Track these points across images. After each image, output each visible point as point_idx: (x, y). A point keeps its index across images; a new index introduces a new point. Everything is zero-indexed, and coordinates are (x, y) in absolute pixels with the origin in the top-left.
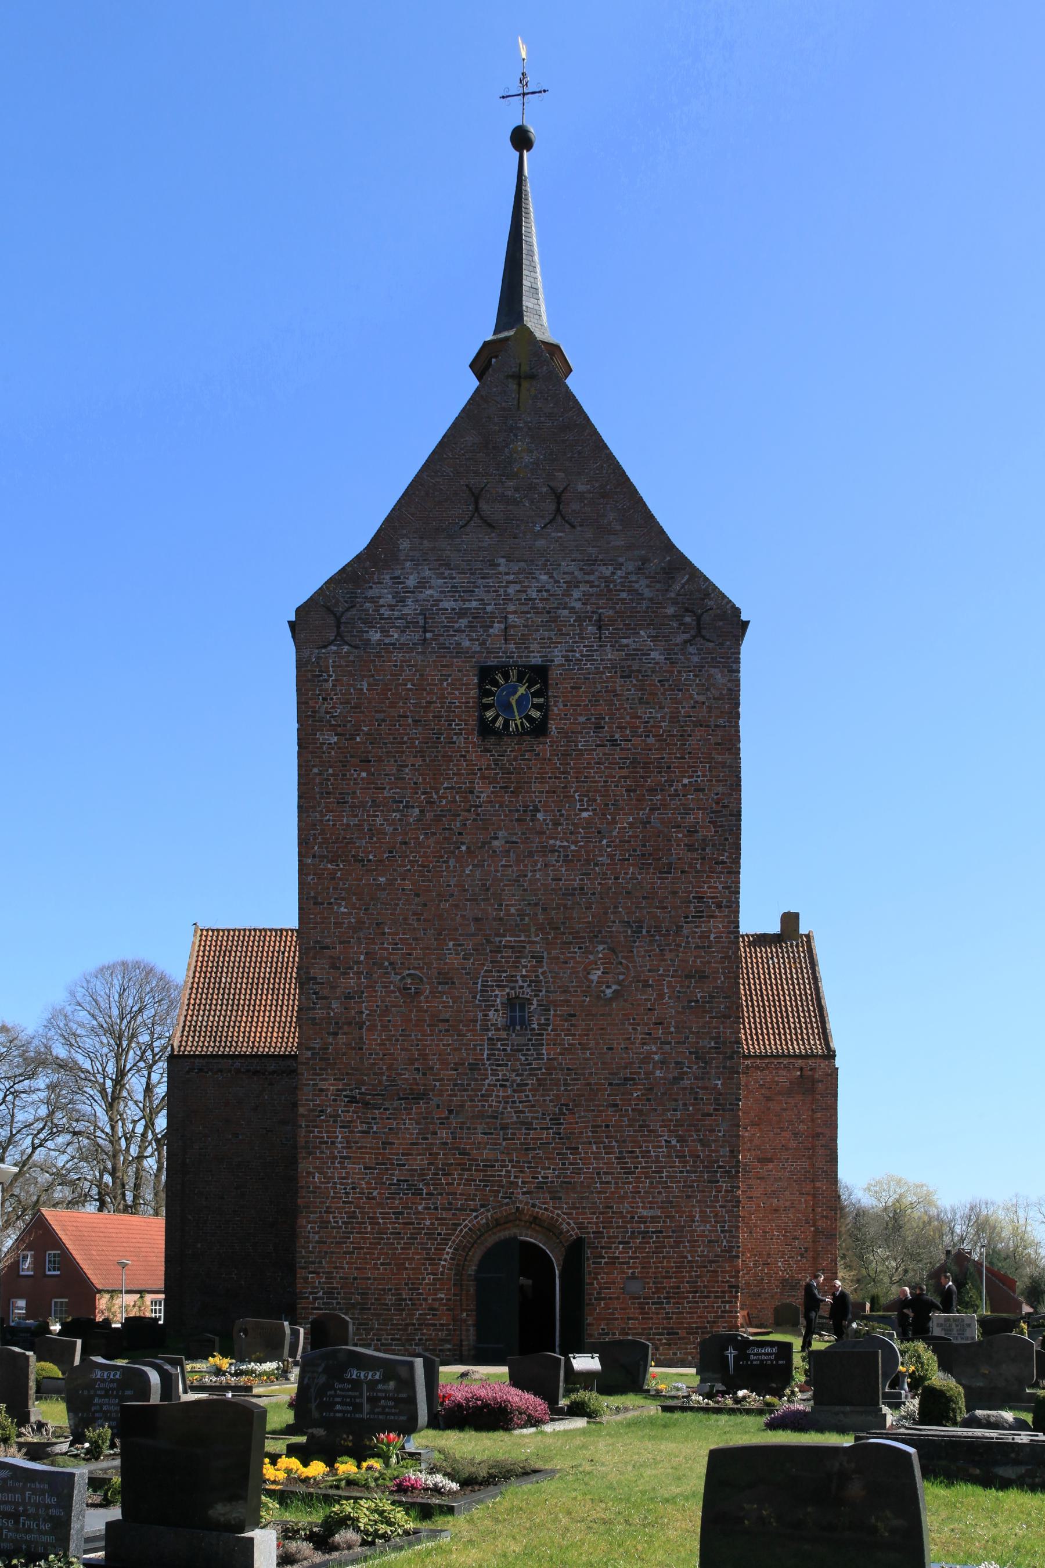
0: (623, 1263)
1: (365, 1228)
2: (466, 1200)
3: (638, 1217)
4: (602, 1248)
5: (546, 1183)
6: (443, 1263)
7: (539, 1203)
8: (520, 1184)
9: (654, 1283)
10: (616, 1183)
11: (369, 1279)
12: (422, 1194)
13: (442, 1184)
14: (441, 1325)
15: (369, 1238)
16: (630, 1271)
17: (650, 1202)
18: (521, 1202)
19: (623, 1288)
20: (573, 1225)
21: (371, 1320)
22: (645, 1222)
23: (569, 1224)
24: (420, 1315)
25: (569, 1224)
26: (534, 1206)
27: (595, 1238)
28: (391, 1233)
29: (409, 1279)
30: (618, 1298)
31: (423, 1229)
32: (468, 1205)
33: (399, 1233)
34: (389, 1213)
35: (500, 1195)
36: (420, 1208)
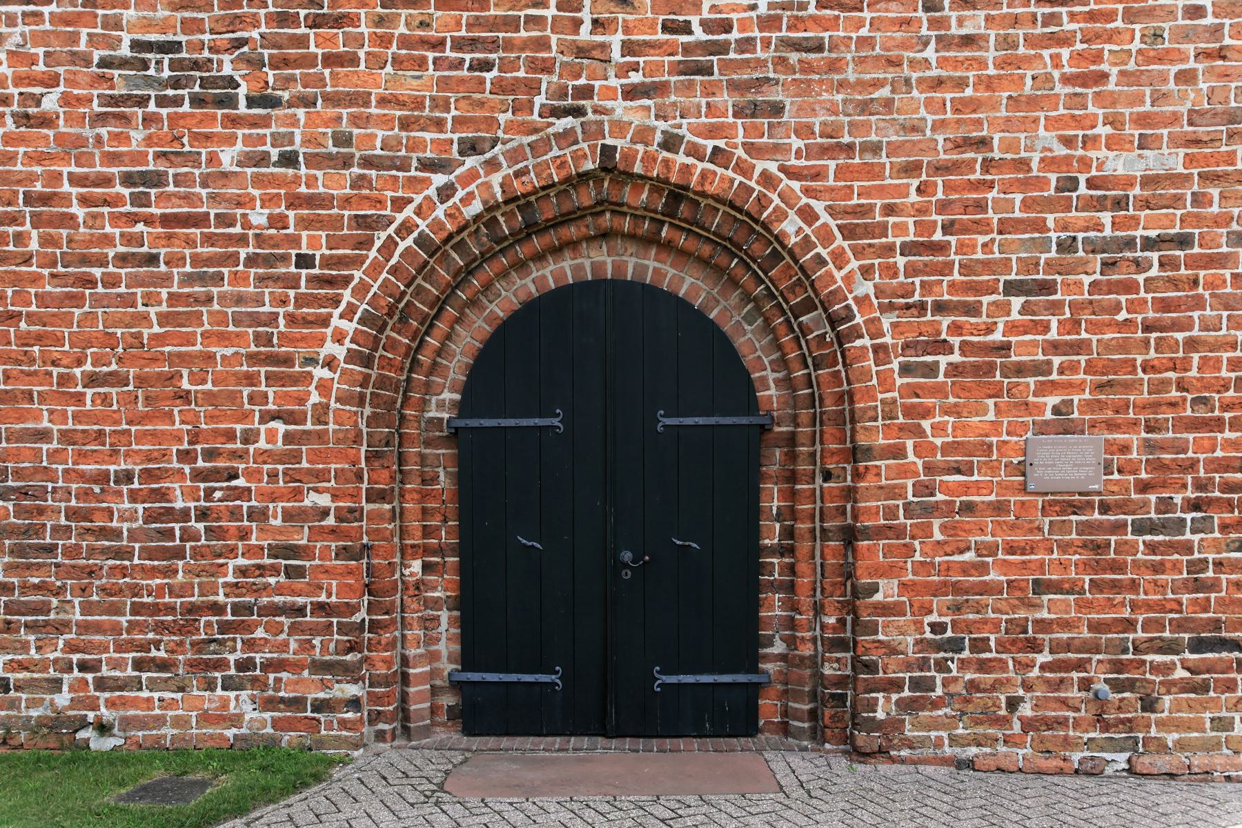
0: (1020, 370)
1: (20, 238)
2: (405, 124)
3: (1091, 184)
4: (940, 308)
5: (722, 48)
6: (320, 373)
7: (694, 130)
8: (616, 54)
9: (1149, 446)
10: (1007, 43)
11: (44, 435)
12: (231, 102)
13: (310, 61)
14: (320, 608)
15: (36, 279)
16: (1052, 400)
17: (1142, 120)
18: (620, 128)
19: (1021, 468)
20: (825, 218)
21: (58, 592)
22: (1120, 204)
23: (808, 215)
24: (242, 571)
25: (808, 215)
26: (671, 142)
27: (911, 271)
28: (123, 259)
29: (195, 438)
30: (999, 508)
31: (242, 240)
32: (414, 146)
33: (152, 259)
34: (107, 181)
35: (539, 100)
36: (228, 158)
